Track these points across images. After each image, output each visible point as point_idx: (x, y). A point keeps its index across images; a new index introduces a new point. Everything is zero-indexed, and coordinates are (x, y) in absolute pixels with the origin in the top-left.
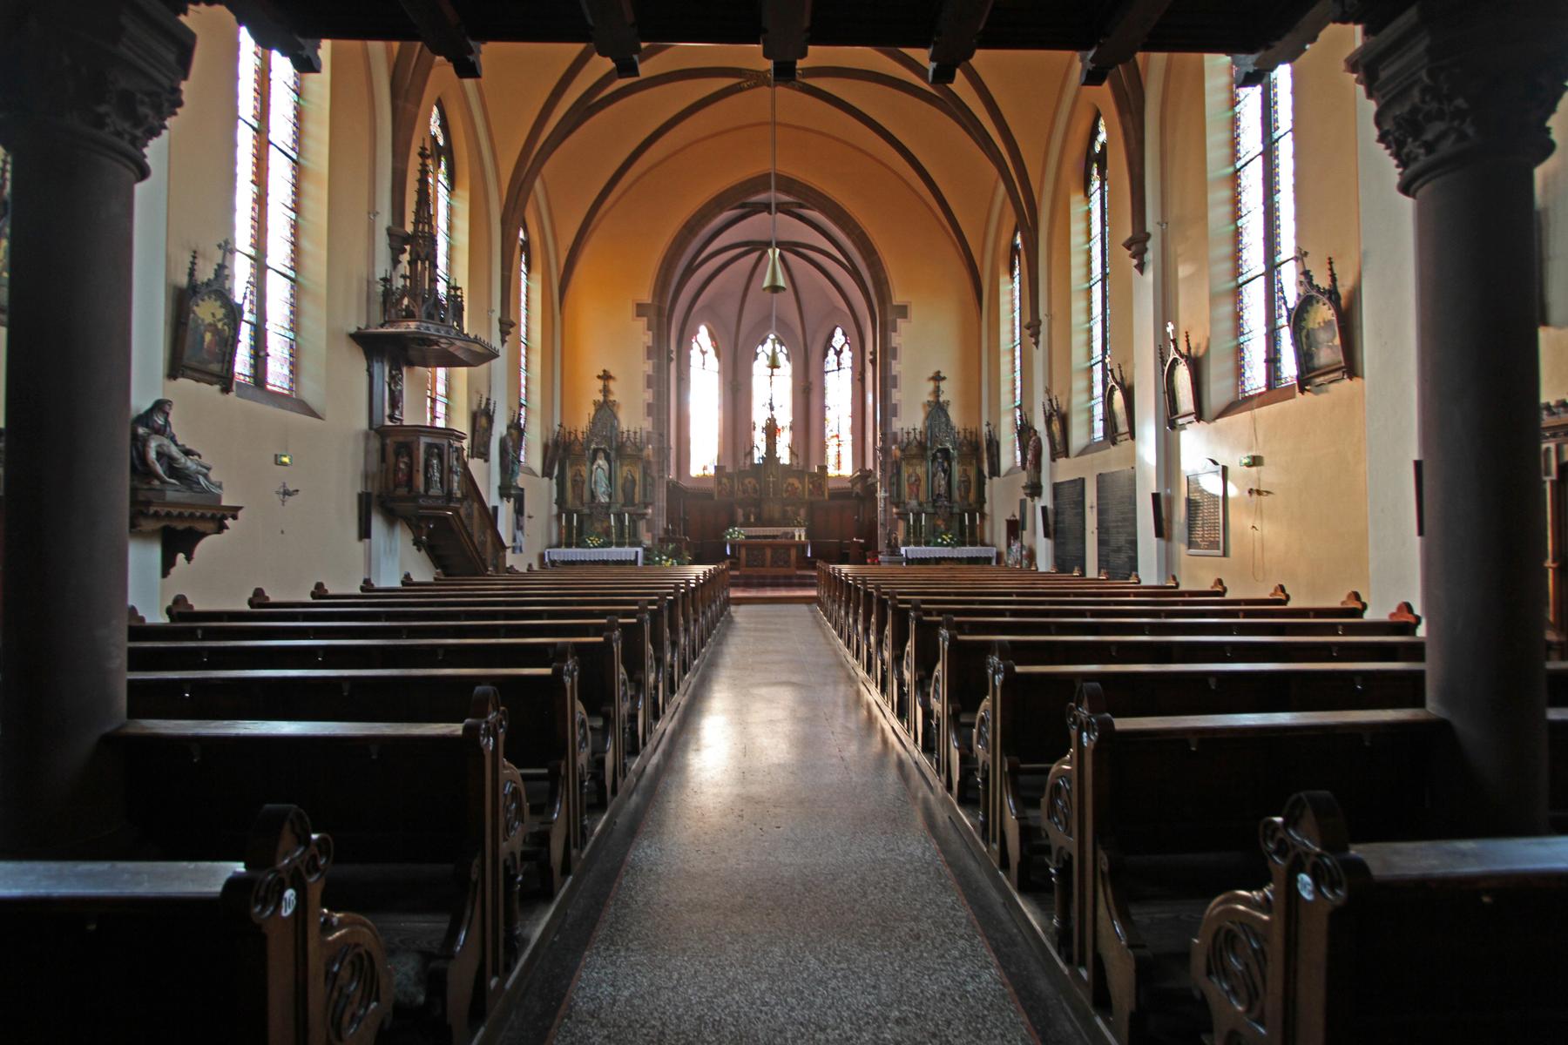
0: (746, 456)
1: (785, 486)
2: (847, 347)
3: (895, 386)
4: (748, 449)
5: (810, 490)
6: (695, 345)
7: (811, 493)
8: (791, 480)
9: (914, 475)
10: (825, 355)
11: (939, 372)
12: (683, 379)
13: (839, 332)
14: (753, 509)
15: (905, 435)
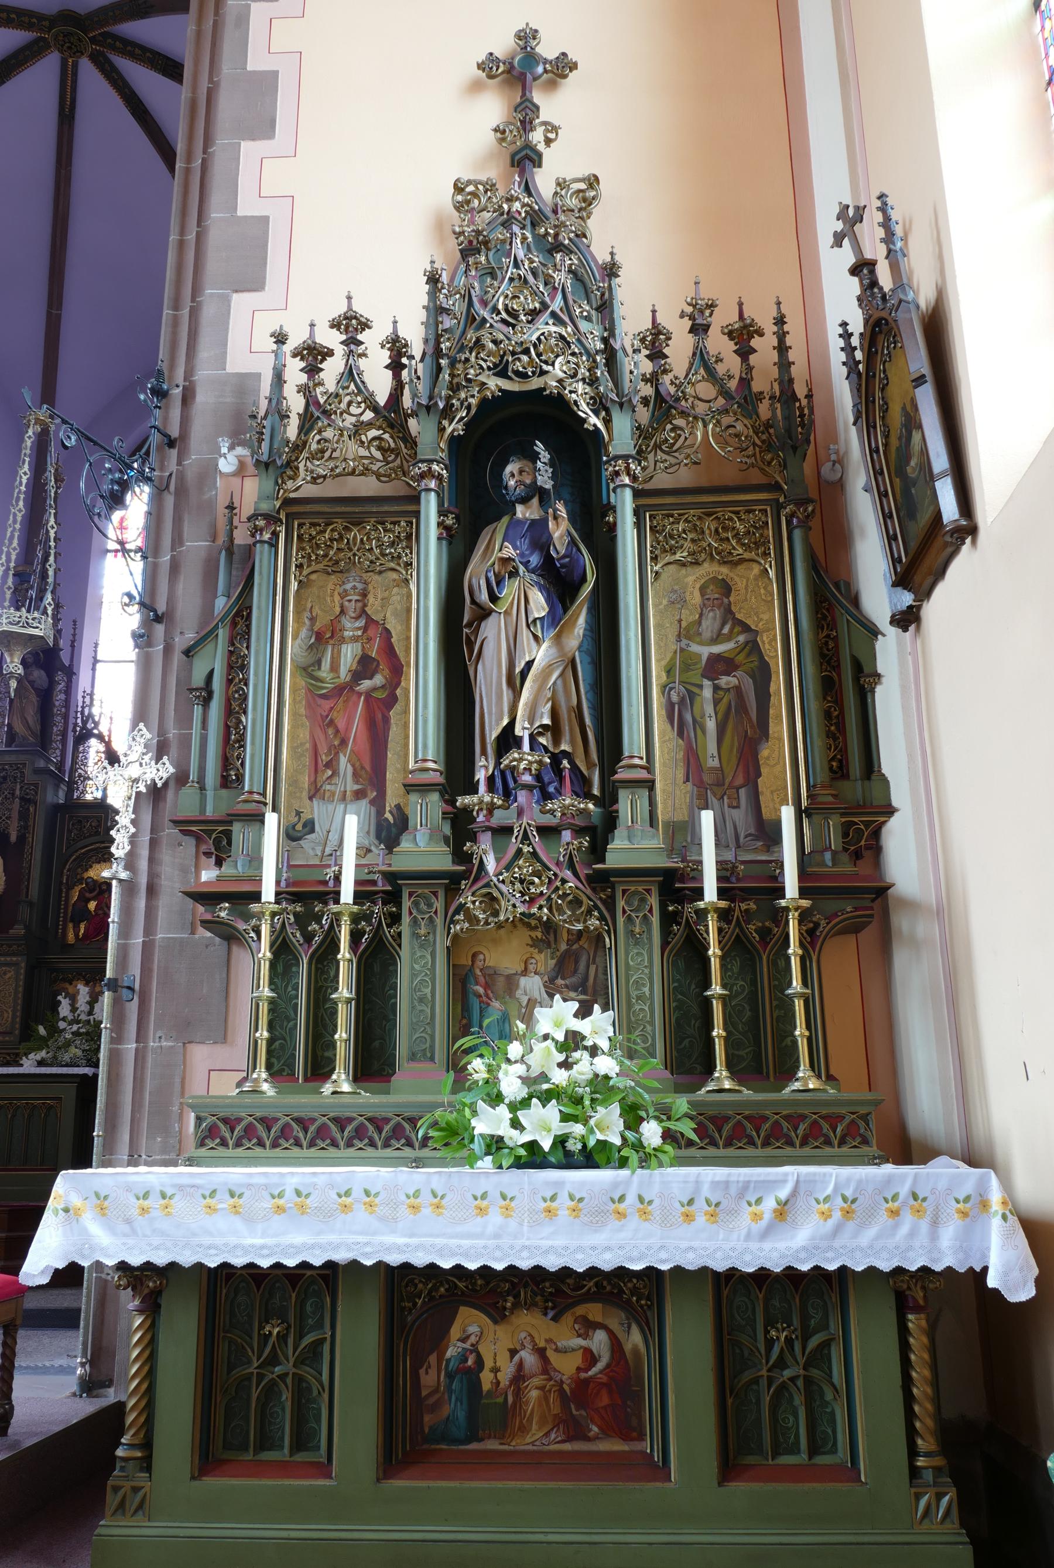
3: (265, 128)
9: (351, 627)
11: (527, 37)
15: (295, 373)
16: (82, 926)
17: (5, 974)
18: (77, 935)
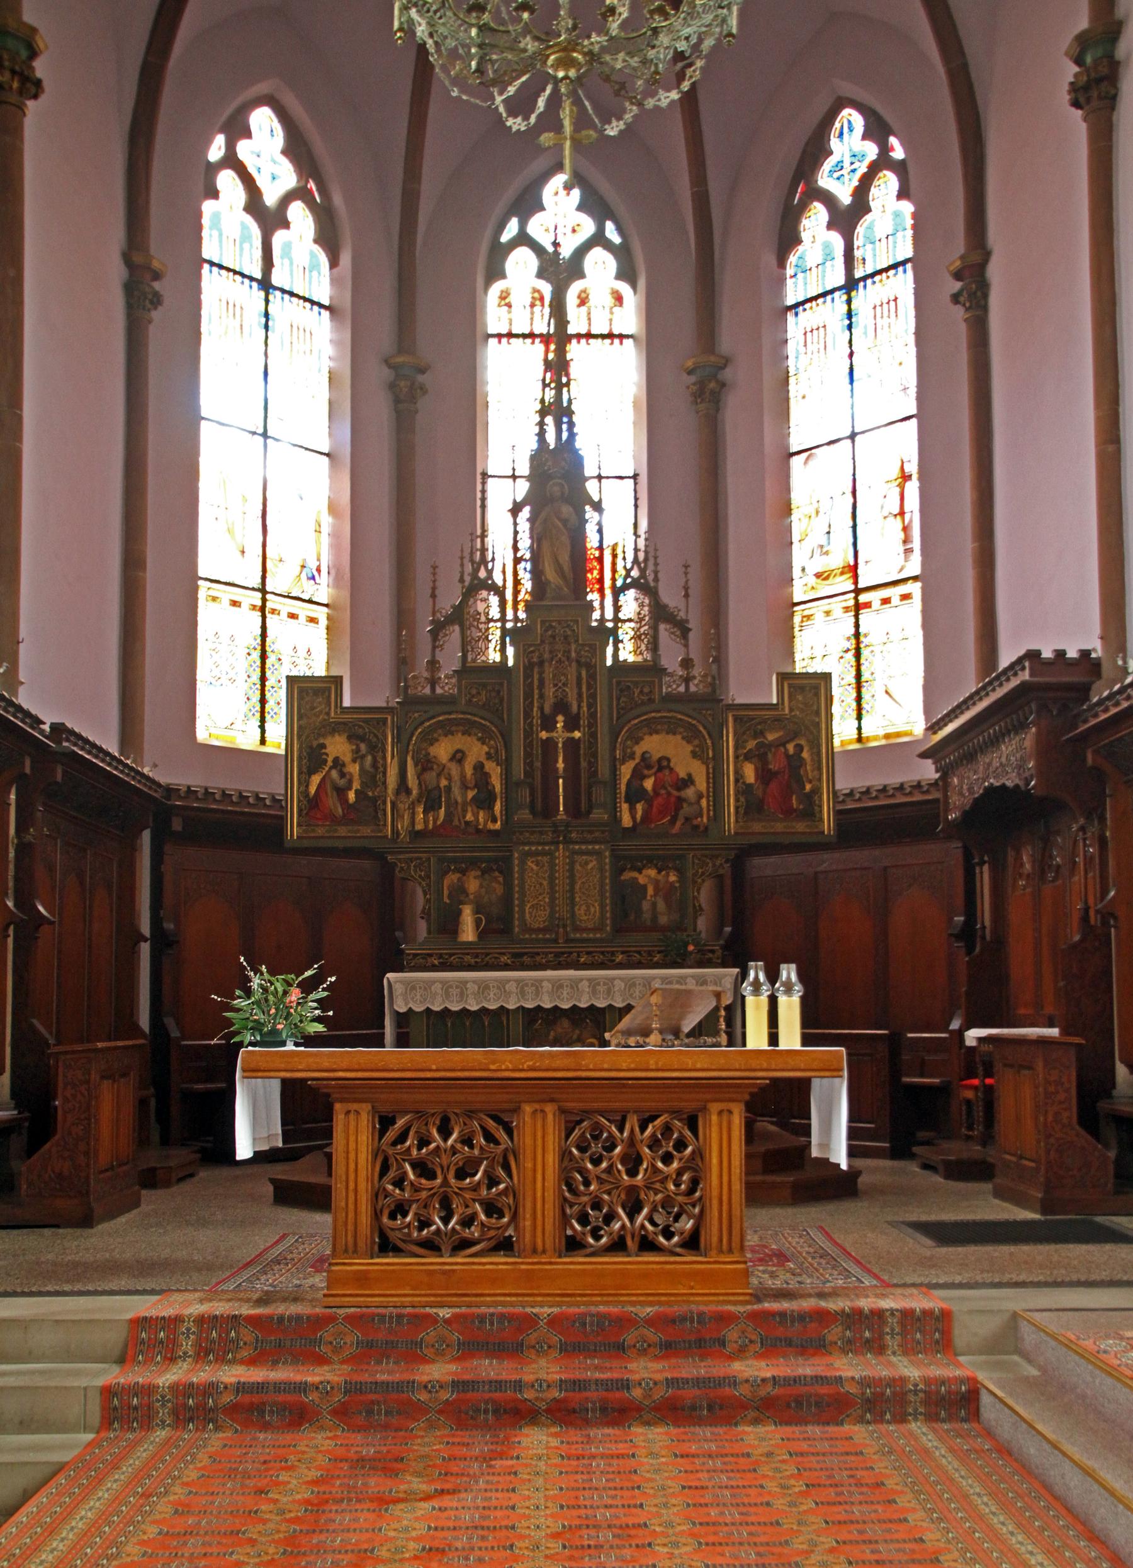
0: (438, 628)
1: (626, 771)
2: (887, 184)
4: (450, 599)
5: (744, 790)
6: (227, 180)
7: (751, 805)
8: (654, 745)
10: (789, 239)
12: (156, 300)
13: (852, 119)
14: (473, 885)
16: (639, 807)
17: (587, 863)
18: (633, 817)
